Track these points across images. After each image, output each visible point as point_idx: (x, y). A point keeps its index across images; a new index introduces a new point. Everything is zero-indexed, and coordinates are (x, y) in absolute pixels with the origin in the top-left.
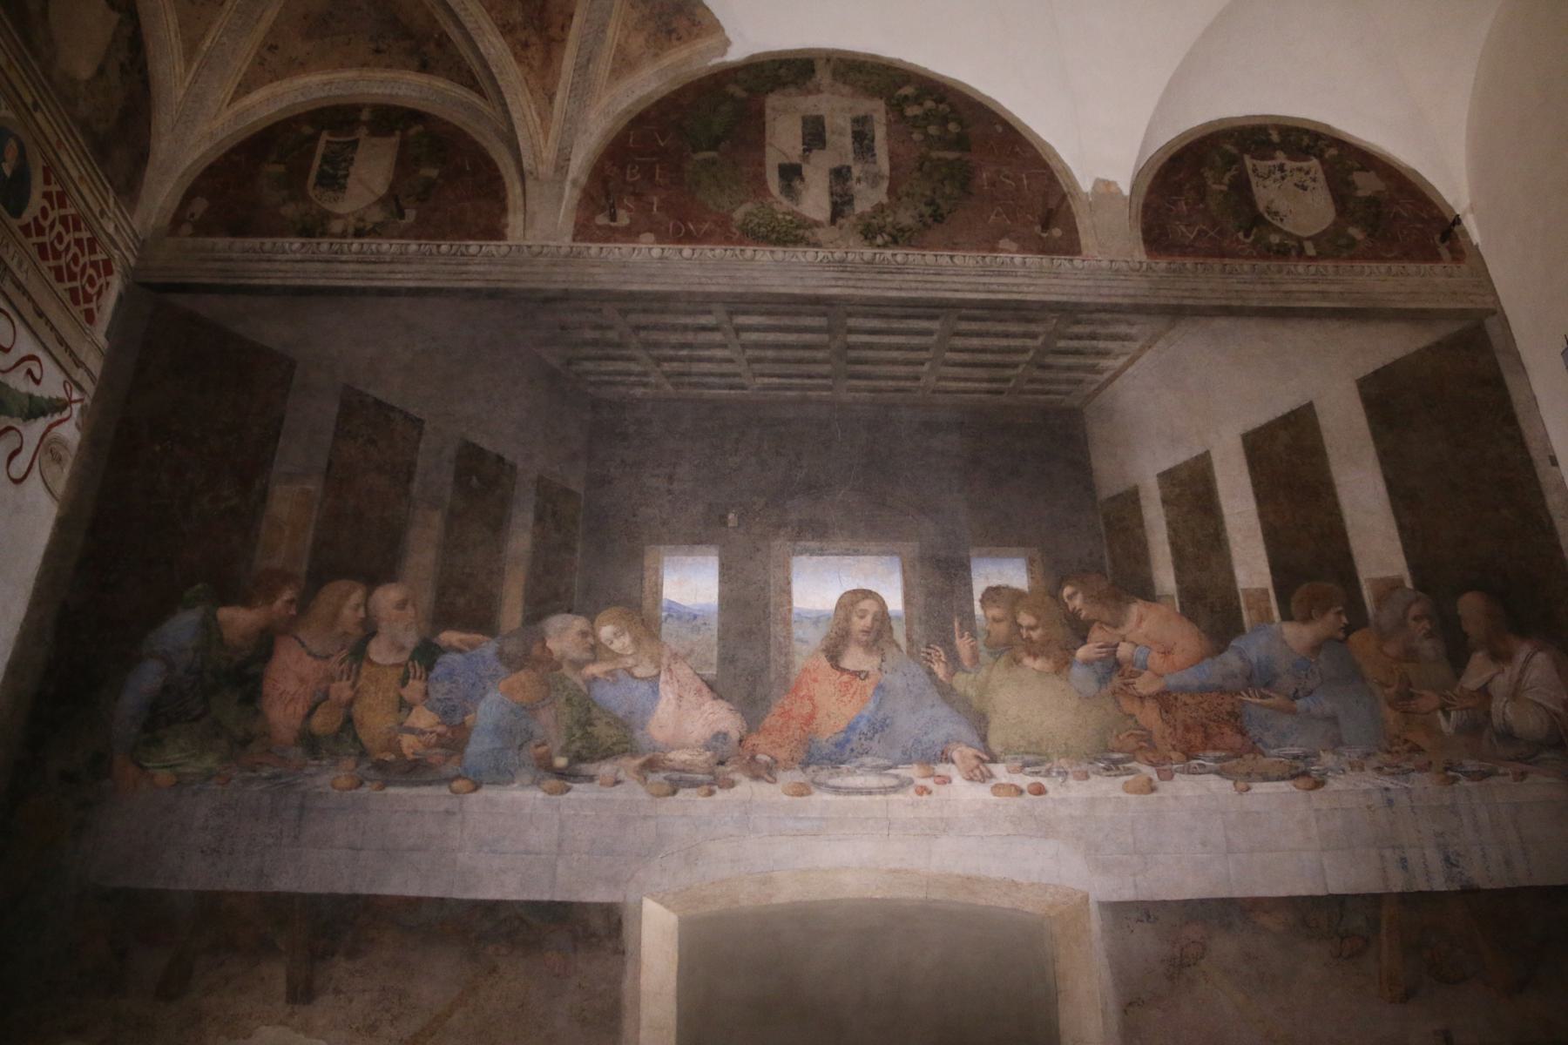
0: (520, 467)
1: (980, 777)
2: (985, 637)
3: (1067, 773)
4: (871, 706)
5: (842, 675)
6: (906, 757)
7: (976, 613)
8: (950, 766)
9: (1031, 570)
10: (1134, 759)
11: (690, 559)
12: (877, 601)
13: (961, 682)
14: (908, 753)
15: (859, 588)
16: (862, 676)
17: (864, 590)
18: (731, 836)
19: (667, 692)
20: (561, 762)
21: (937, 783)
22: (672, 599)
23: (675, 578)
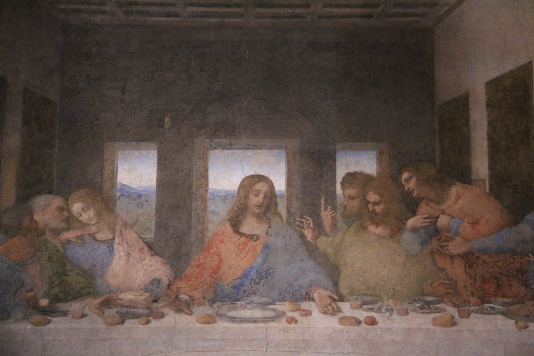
0: (9, 81)
1: (332, 311)
2: (342, 210)
3: (392, 310)
4: (260, 260)
5: (240, 237)
6: (282, 296)
7: (337, 193)
8: (311, 303)
9: (380, 160)
10: (442, 301)
11: (137, 153)
12: (268, 183)
13: (323, 243)
14: (283, 294)
15: (256, 174)
16: (254, 238)
17: (258, 175)
18: (161, 352)
19: (120, 251)
20: (44, 302)
21: (302, 315)
22: (124, 182)
23: (126, 167)
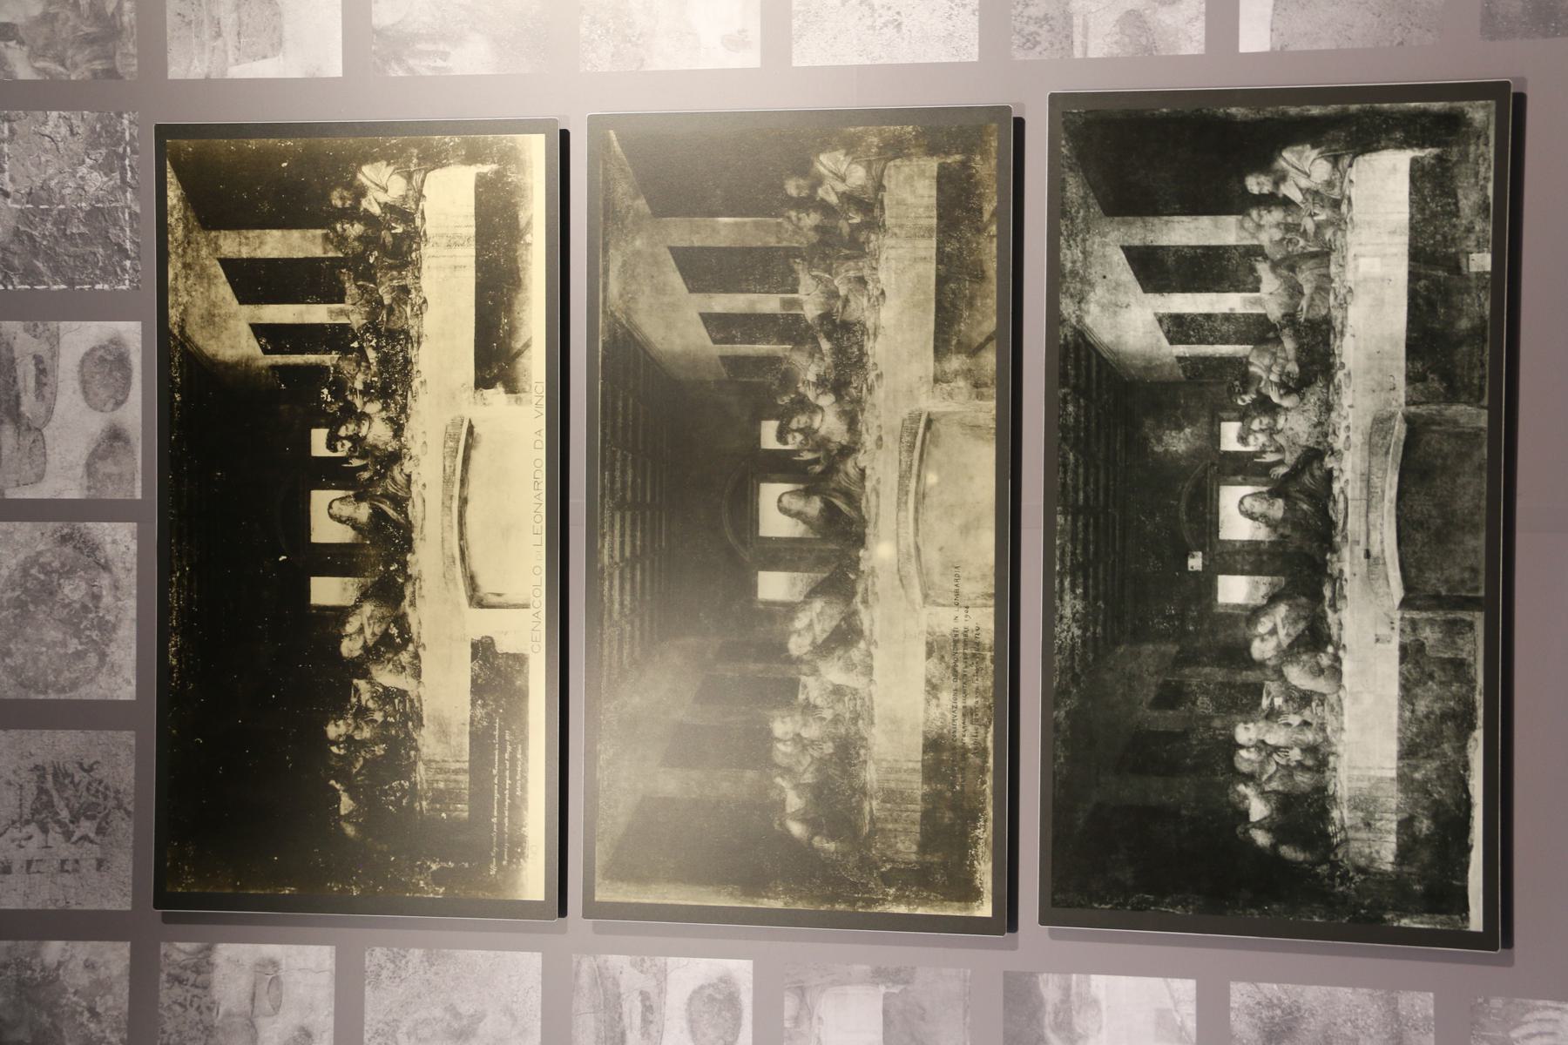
21: (276, 1009)
